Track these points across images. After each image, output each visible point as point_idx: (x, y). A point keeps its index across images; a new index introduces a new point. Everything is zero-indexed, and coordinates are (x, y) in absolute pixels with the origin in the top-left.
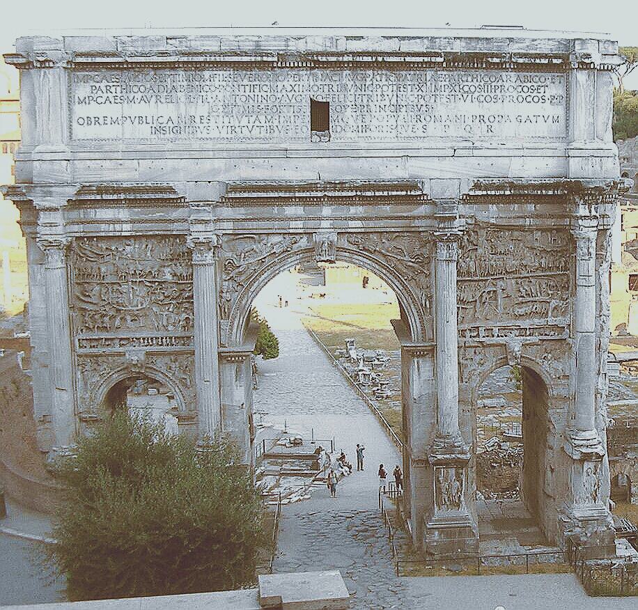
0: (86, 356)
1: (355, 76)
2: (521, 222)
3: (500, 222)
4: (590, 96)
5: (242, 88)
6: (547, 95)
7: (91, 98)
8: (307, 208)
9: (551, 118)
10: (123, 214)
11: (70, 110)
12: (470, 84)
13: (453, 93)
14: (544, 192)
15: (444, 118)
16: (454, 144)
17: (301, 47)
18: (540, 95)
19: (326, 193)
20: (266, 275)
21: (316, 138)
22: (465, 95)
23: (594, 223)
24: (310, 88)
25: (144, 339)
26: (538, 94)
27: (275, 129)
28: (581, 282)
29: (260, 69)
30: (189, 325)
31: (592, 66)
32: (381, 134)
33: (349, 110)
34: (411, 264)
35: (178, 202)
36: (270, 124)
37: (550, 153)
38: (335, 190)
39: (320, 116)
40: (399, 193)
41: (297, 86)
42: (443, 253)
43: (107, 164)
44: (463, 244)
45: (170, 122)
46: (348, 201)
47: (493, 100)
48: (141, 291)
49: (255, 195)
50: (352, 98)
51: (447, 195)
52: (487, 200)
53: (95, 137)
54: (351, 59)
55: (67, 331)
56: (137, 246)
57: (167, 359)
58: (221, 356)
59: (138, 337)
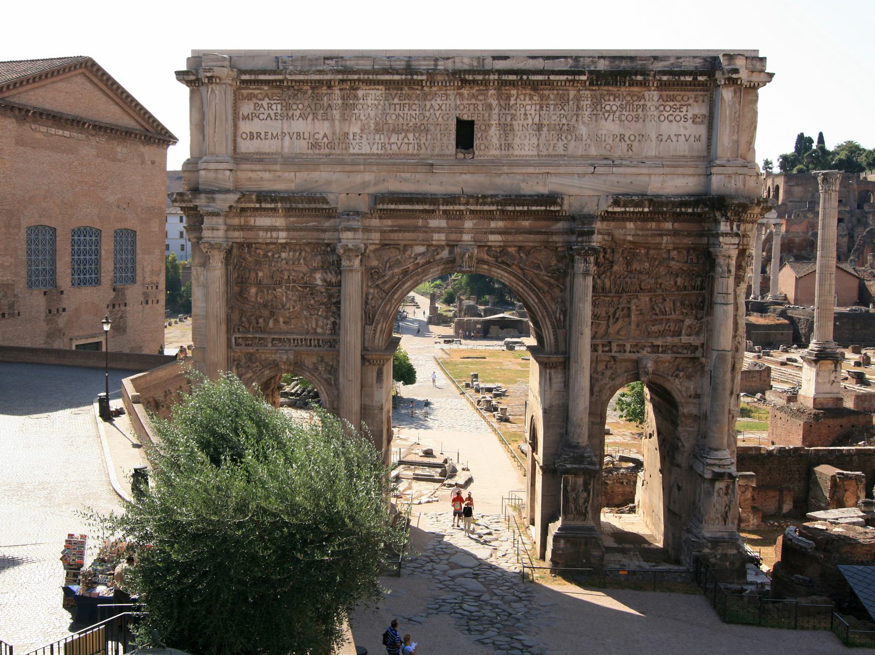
1: (499, 97)
3: (640, 240)
4: (735, 113)
5: (393, 107)
6: (690, 115)
7: (254, 115)
8: (450, 222)
9: (692, 138)
10: (280, 222)
11: (235, 126)
12: (612, 103)
13: (595, 112)
14: (683, 210)
15: (585, 137)
16: (593, 162)
17: (449, 65)
18: (682, 114)
19: (469, 207)
20: (409, 284)
21: (460, 156)
22: (606, 115)
23: (736, 240)
24: (457, 107)
25: (294, 340)
26: (680, 113)
27: (423, 145)
28: (719, 299)
29: (410, 88)
30: (335, 328)
31: (739, 82)
32: (523, 153)
33: (493, 128)
34: (547, 278)
35: (331, 213)
36: (418, 141)
38: (477, 204)
40: (538, 208)
41: (444, 105)
42: (580, 266)
43: (267, 175)
44: (599, 261)
45: (325, 139)
46: (490, 216)
47: (634, 119)
49: (401, 207)
50: (495, 117)
51: (586, 211)
52: (622, 218)
53: (257, 151)
54: (496, 77)
55: (224, 328)
56: (291, 253)
58: (363, 358)
59: (289, 337)
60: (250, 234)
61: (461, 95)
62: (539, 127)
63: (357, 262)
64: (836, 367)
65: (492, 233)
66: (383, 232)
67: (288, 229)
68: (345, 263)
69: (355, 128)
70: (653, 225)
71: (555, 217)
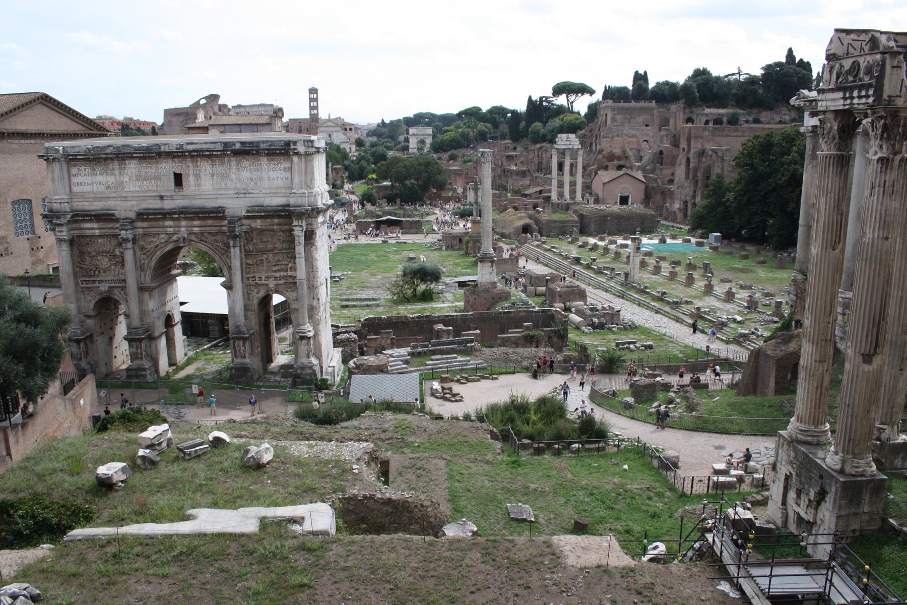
0: (84, 288)
1: (192, 162)
2: (272, 227)
3: (264, 228)
6: (282, 168)
10: (95, 225)
17: (167, 149)
21: (177, 190)
24: (173, 167)
28: (297, 256)
35: (117, 220)
37: (282, 195)
39: (178, 180)
43: (86, 203)
46: (192, 219)
48: (106, 259)
50: (191, 171)
55: (72, 277)
57: (119, 290)
60: (82, 232)
61: (174, 161)
62: (213, 175)
63: (130, 245)
64: (492, 264)
65: (194, 227)
66: (143, 228)
67: (99, 229)
68: (124, 245)
69: (126, 179)
70: (269, 220)
71: (223, 218)
